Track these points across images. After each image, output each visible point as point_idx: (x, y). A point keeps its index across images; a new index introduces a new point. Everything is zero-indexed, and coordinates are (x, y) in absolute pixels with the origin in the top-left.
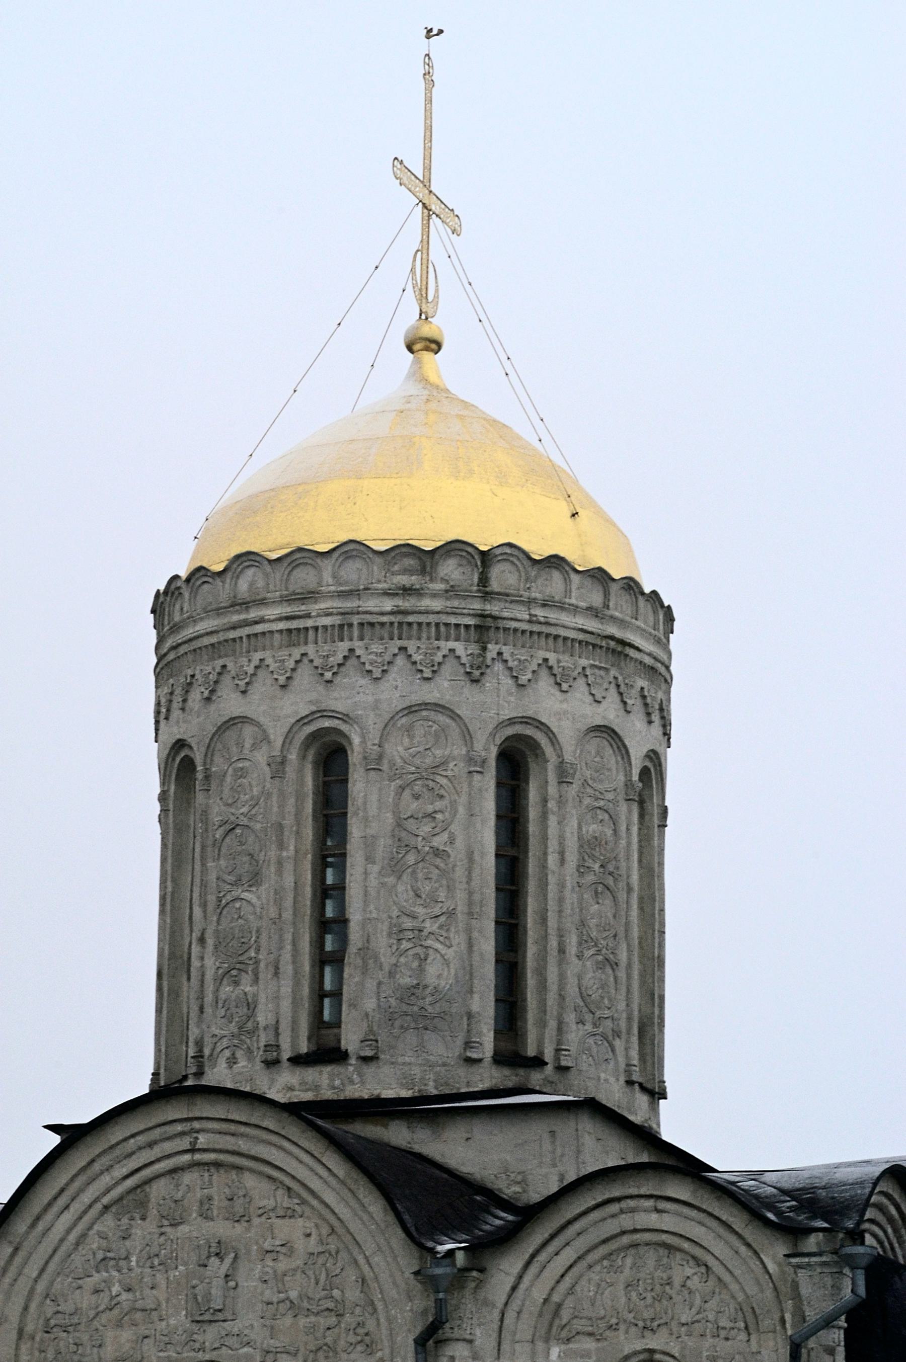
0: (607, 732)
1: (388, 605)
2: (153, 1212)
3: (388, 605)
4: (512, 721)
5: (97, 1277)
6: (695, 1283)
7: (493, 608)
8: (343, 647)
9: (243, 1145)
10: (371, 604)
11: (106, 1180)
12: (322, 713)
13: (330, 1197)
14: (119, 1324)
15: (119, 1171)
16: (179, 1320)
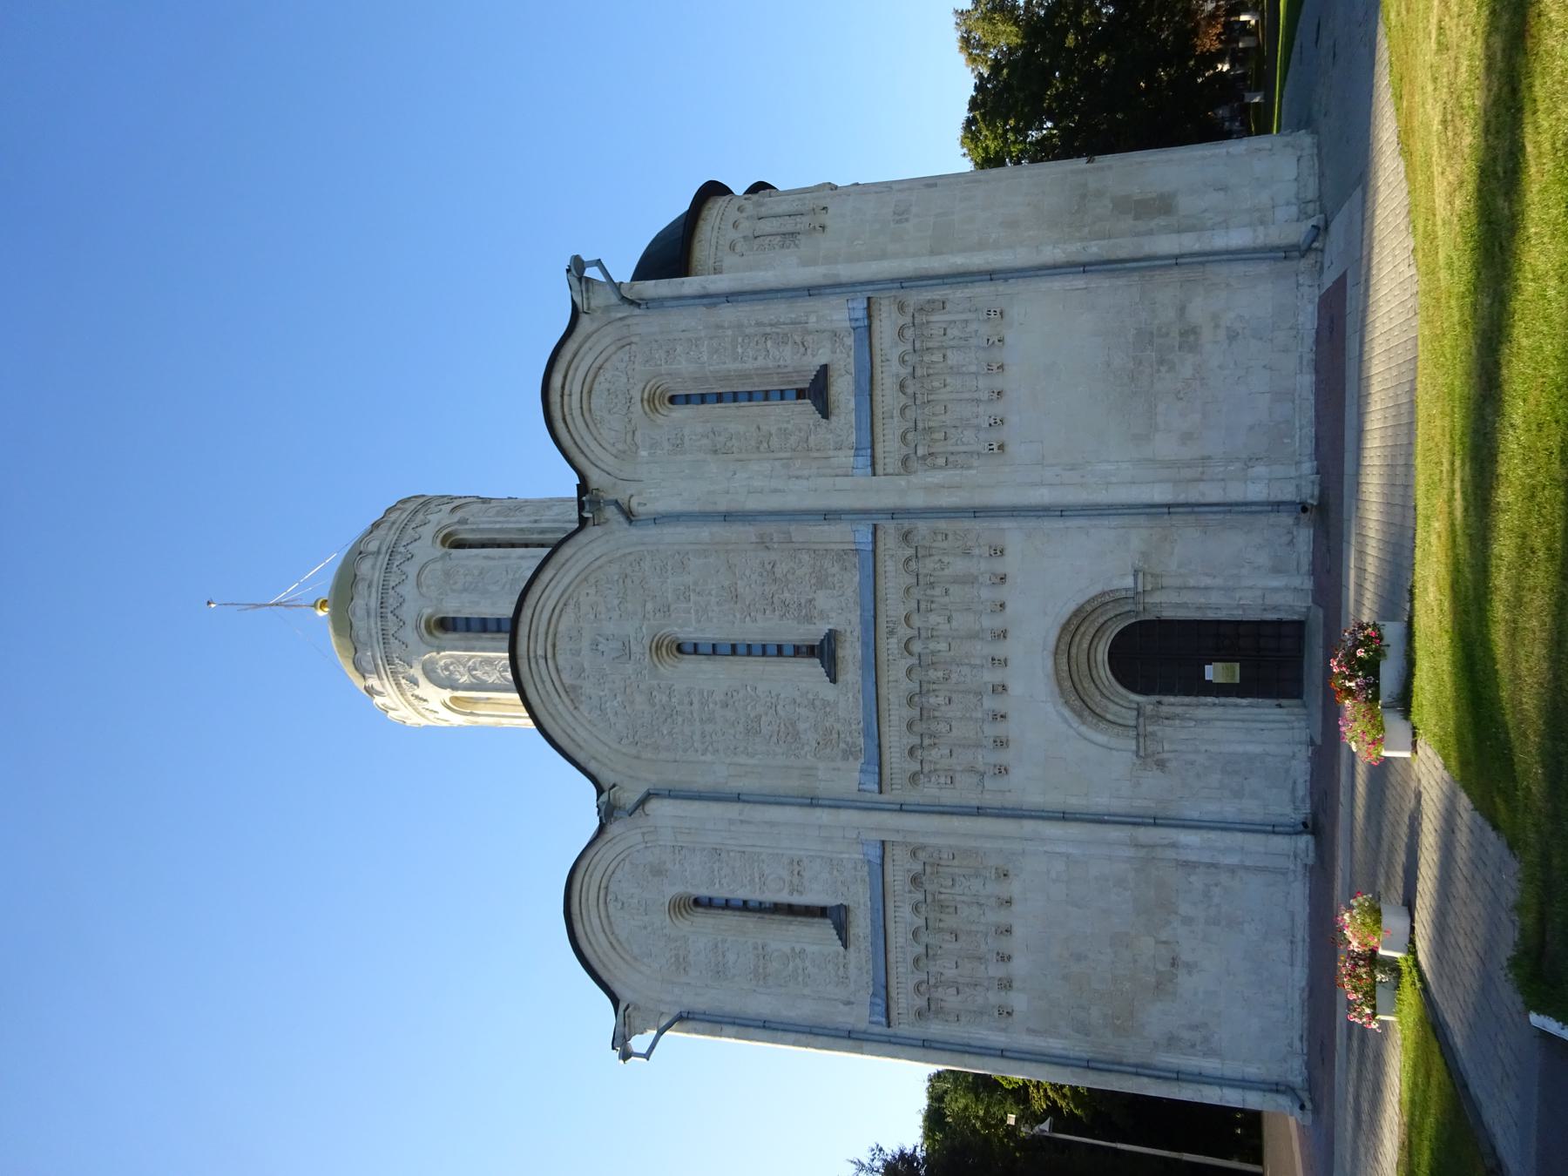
0: (453, 510)
1: (374, 595)
2: (578, 682)
3: (374, 595)
4: (434, 542)
5: (610, 715)
6: (608, 376)
7: (384, 549)
8: (390, 615)
9: (542, 630)
10: (374, 603)
11: (560, 707)
12: (417, 627)
13: (566, 581)
14: (632, 702)
15: (557, 700)
16: (629, 668)
